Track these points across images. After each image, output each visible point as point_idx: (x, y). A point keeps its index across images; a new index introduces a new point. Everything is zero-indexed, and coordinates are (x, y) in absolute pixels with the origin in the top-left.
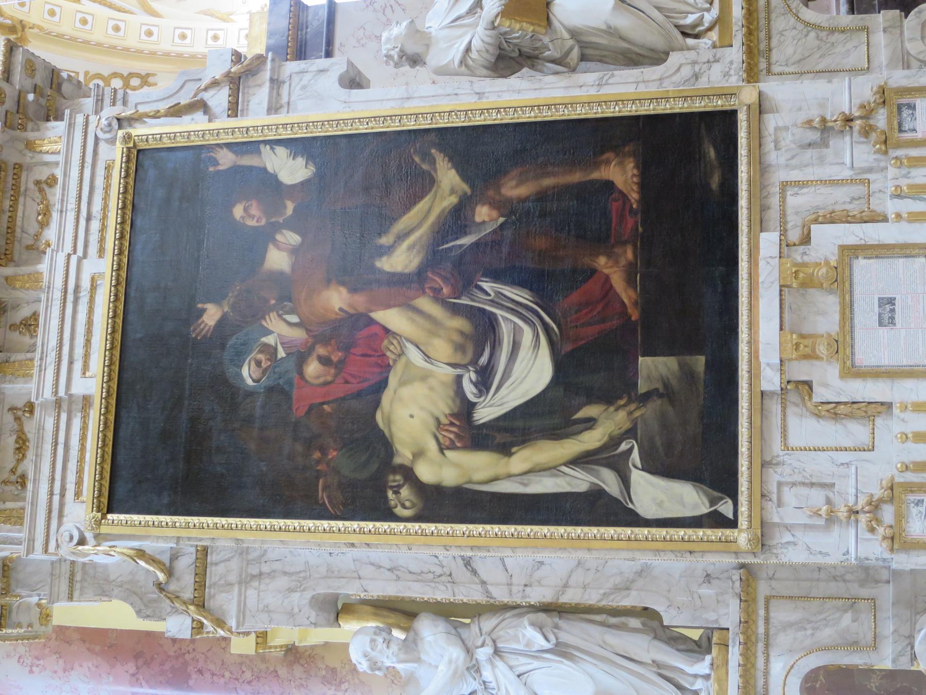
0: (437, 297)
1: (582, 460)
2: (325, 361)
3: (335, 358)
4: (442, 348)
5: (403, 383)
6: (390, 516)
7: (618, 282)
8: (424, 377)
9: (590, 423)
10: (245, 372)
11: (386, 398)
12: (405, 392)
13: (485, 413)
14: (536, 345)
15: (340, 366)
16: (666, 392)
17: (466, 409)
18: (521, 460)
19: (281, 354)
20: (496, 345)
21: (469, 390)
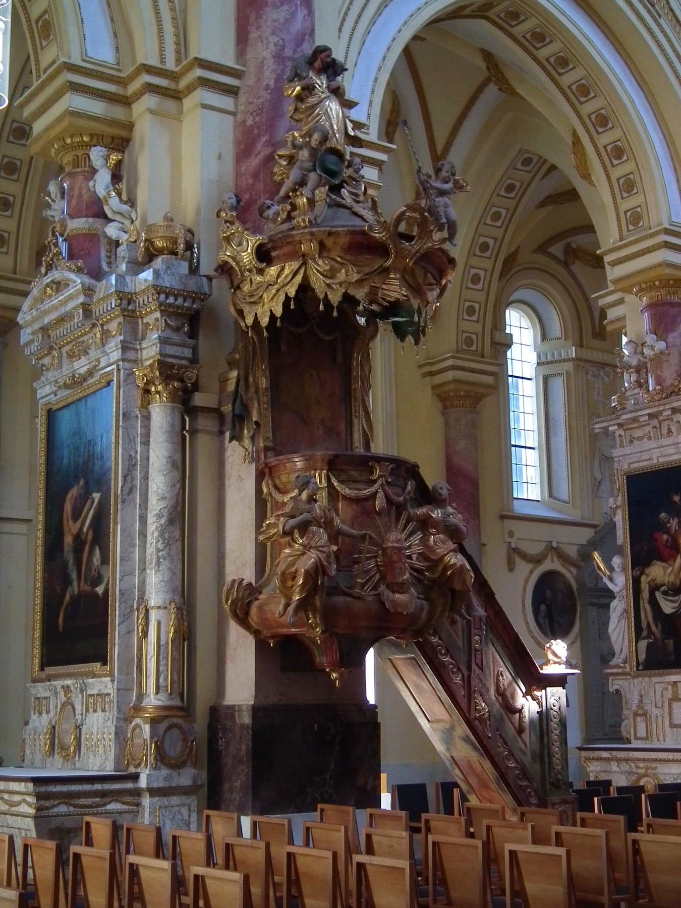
1: (649, 625)
2: (667, 540)
3: (668, 544)
4: (672, 578)
5: (663, 567)
6: (633, 569)
8: (665, 574)
9: (657, 626)
10: (663, 514)
11: (659, 563)
12: (661, 568)
13: (658, 595)
14: (674, 608)
15: (666, 546)
18: (648, 607)
19: (668, 525)
20: (674, 596)
21: (662, 589)
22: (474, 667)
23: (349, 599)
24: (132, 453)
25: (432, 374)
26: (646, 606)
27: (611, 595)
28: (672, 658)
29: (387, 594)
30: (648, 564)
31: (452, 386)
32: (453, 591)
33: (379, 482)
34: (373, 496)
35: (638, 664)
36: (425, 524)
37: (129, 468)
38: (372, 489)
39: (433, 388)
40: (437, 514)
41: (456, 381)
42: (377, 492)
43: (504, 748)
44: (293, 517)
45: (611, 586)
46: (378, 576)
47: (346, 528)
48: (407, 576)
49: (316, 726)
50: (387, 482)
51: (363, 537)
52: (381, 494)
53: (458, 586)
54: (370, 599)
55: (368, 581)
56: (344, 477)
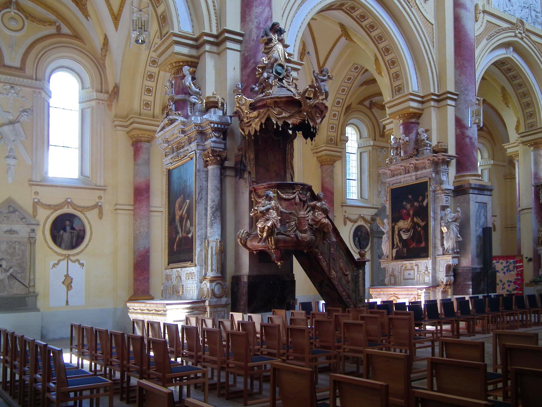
0: (412, 225)
1: (397, 244)
4: (407, 226)
7: (413, 245)
9: (400, 244)
13: (401, 232)
16: (403, 251)
17: (401, 230)
18: (397, 237)
20: (407, 232)
21: (403, 230)
23: (284, 236)
25: (316, 153)
26: (396, 237)
27: (383, 233)
28: (405, 255)
29: (300, 235)
30: (398, 221)
31: (324, 157)
32: (324, 232)
33: (297, 193)
34: (295, 198)
35: (392, 258)
36: (314, 208)
38: (294, 196)
39: (317, 158)
40: (319, 204)
41: (326, 155)
44: (264, 207)
45: (383, 230)
46: (295, 228)
47: (284, 210)
48: (307, 227)
50: (300, 193)
51: (291, 213)
52: (297, 197)
53: (326, 231)
54: (293, 236)
55: (292, 229)
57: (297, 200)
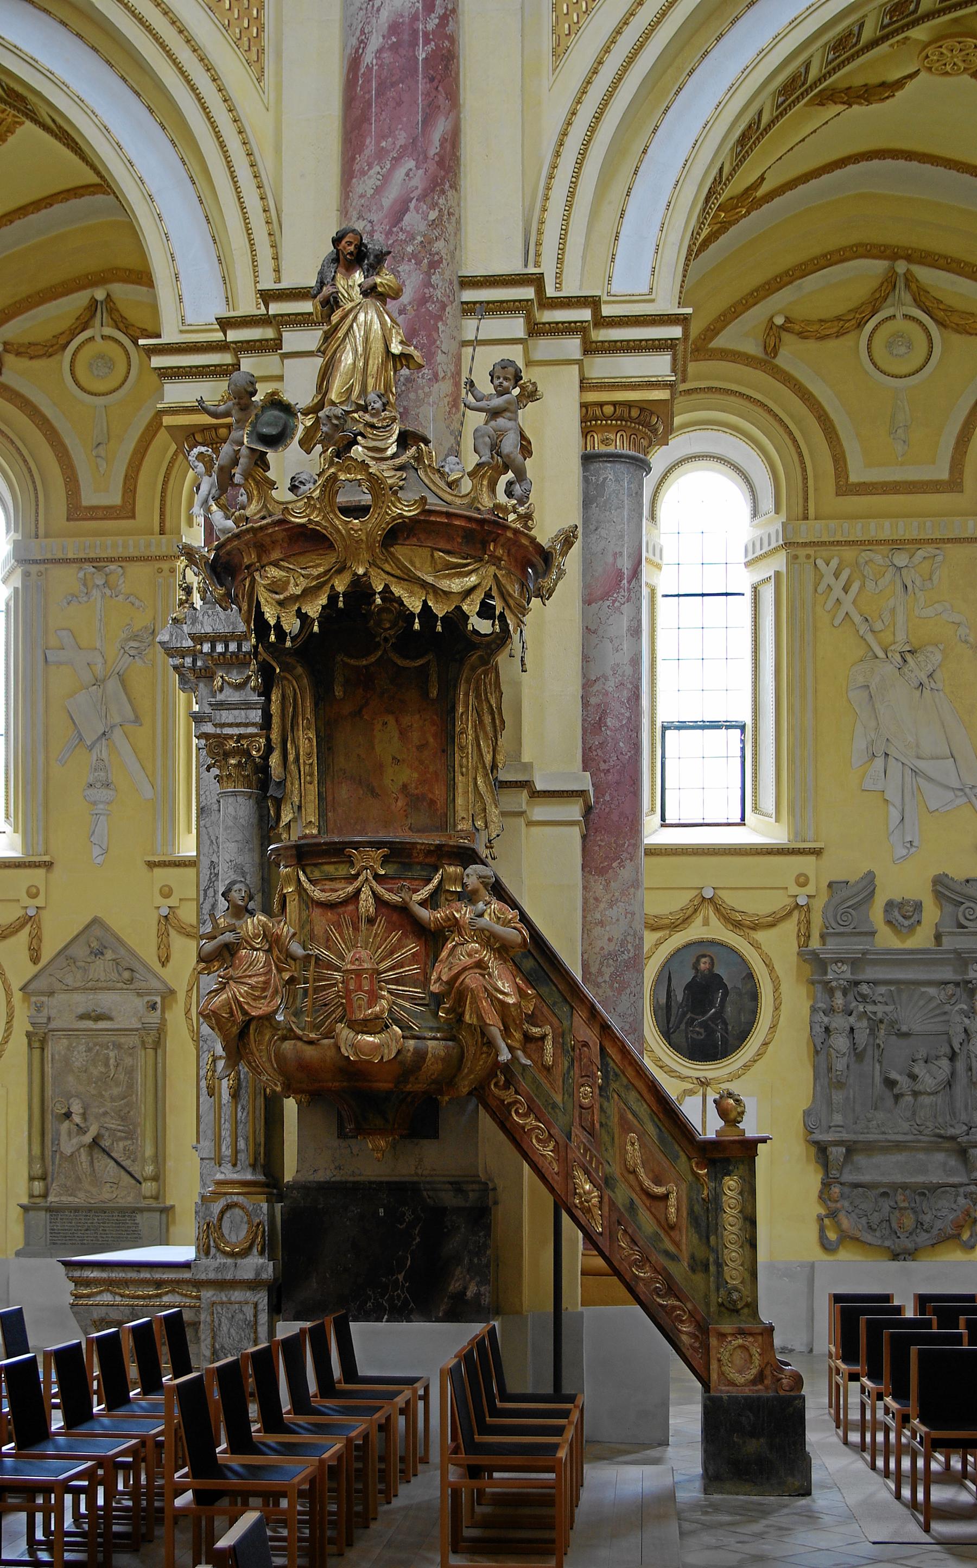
22: (576, 1130)
24: (215, 859)
33: (361, 878)
37: (210, 879)
38: (350, 889)
42: (358, 891)
43: (632, 1249)
49: (381, 1210)
56: (317, 874)
57: (366, 903)
